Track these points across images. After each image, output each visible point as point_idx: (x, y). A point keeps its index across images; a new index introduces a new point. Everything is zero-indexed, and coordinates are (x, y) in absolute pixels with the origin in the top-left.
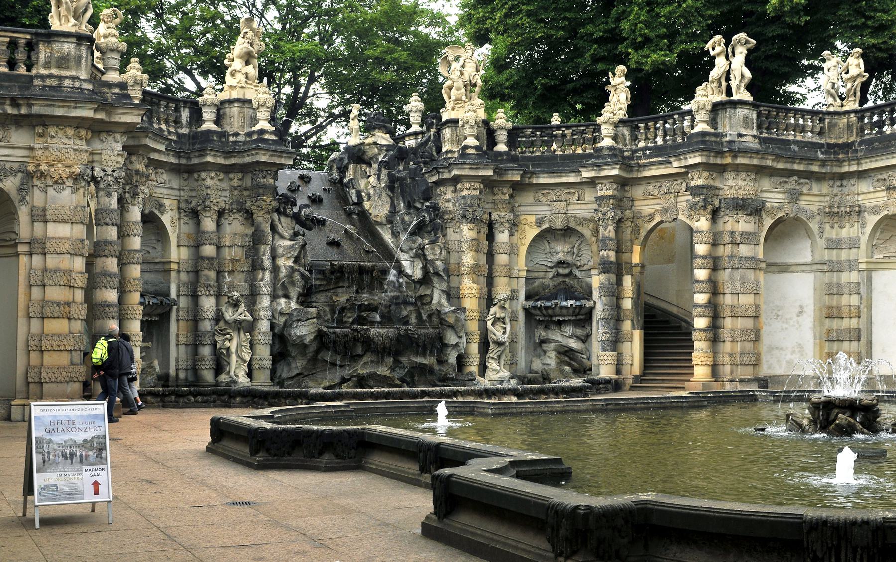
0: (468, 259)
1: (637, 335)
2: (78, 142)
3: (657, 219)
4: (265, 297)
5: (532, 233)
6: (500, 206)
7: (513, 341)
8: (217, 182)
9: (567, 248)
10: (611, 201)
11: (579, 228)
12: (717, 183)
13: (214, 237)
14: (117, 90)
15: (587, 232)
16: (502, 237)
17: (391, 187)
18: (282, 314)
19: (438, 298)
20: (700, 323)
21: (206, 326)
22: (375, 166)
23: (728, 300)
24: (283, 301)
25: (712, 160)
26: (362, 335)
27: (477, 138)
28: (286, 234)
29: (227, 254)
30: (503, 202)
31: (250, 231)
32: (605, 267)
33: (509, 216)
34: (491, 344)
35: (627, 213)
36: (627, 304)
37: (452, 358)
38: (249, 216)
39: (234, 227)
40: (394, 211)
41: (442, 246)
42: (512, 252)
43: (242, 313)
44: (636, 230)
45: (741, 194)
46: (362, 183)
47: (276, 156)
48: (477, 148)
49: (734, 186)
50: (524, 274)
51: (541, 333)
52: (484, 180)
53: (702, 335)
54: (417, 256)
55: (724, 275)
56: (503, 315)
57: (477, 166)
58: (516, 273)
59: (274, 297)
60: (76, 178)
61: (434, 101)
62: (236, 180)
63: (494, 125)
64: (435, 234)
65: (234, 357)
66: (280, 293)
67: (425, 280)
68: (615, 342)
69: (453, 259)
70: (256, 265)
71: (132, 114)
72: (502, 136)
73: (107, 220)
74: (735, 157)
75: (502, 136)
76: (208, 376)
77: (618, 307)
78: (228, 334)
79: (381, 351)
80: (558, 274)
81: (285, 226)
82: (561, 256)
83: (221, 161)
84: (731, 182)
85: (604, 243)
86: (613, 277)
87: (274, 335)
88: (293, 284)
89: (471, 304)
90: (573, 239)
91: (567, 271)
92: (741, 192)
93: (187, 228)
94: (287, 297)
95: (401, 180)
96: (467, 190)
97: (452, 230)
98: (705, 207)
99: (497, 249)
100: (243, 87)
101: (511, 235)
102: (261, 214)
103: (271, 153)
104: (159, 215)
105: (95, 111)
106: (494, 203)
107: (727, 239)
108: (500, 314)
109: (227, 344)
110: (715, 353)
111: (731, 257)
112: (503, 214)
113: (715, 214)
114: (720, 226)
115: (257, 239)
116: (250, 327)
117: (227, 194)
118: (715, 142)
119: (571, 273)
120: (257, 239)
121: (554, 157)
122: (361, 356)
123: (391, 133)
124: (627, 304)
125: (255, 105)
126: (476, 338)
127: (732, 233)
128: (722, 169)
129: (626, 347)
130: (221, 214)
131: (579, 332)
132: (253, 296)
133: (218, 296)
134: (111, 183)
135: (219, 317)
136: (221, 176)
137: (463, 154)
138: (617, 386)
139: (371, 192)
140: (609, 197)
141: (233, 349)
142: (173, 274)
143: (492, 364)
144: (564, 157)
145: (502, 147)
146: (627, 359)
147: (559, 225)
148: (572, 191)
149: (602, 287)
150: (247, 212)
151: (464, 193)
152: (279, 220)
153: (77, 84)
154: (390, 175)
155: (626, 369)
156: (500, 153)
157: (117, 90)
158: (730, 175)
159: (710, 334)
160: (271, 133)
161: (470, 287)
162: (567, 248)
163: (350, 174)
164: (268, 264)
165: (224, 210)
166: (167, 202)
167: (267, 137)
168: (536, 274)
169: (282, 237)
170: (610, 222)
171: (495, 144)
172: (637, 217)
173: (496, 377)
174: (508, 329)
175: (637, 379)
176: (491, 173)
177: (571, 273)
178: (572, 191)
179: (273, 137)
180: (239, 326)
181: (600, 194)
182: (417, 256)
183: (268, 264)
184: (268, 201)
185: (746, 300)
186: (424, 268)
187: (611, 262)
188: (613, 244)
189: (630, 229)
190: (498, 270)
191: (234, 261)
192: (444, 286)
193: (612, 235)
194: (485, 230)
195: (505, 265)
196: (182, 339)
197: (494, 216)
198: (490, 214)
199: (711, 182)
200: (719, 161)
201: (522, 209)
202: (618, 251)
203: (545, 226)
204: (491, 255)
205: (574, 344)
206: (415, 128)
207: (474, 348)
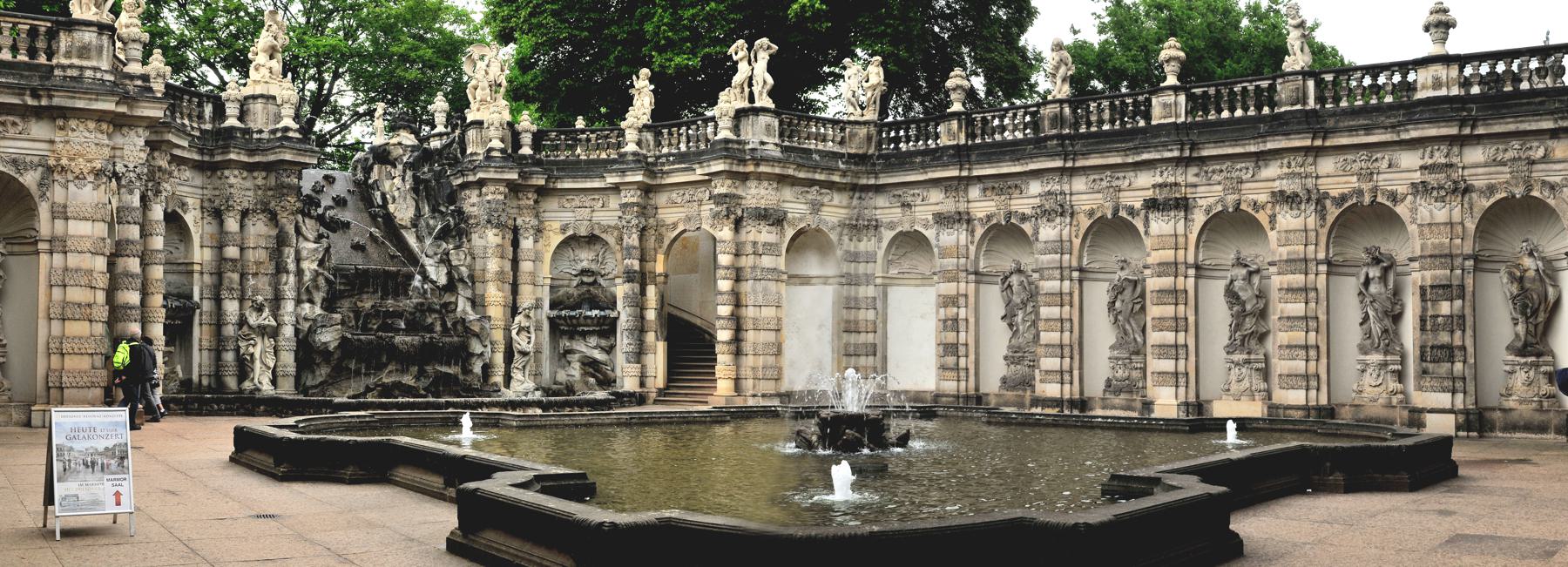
0: (493, 265)
1: (661, 347)
3: (681, 228)
5: (557, 239)
7: (538, 352)
9: (591, 255)
11: (603, 236)
12: (740, 192)
13: (238, 237)
15: (611, 240)
16: (527, 243)
17: (415, 190)
18: (306, 319)
19: (463, 305)
20: (724, 335)
21: (230, 330)
22: (400, 167)
23: (749, 312)
24: (307, 306)
27: (502, 140)
28: (311, 237)
29: (251, 256)
30: (528, 207)
31: (274, 232)
32: (630, 276)
33: (534, 222)
35: (651, 221)
36: (651, 315)
38: (273, 218)
39: (259, 229)
40: (418, 215)
42: (537, 259)
43: (266, 319)
44: (660, 239)
45: (763, 204)
46: (387, 185)
48: (503, 151)
49: (757, 195)
50: (548, 281)
51: (565, 343)
52: (510, 184)
53: (725, 348)
54: (441, 261)
55: (747, 287)
57: (501, 169)
59: (298, 302)
61: (459, 102)
63: (519, 127)
65: (258, 364)
66: (304, 297)
67: (451, 287)
68: (639, 354)
69: (479, 265)
70: (280, 269)
72: (527, 139)
75: (527, 139)
76: (232, 382)
77: (642, 317)
79: (404, 359)
80: (583, 283)
81: (310, 228)
82: (585, 264)
85: (628, 253)
86: (637, 287)
87: (299, 342)
88: (317, 288)
89: (496, 312)
90: (598, 247)
91: (591, 280)
93: (211, 228)
94: (311, 301)
95: (427, 181)
96: (493, 194)
98: (728, 217)
99: (521, 255)
101: (536, 241)
106: (519, 208)
107: (749, 249)
108: (525, 323)
109: (251, 350)
110: (738, 367)
111: (754, 268)
113: (738, 224)
114: (743, 236)
115: (281, 240)
116: (274, 333)
117: (250, 193)
119: (595, 282)
120: (281, 240)
121: (579, 162)
123: (416, 133)
124: (651, 315)
126: (501, 347)
127: (755, 243)
129: (649, 359)
130: (245, 214)
131: (603, 343)
132: (277, 300)
133: (242, 300)
135: (242, 322)
136: (245, 174)
137: (488, 158)
138: (641, 399)
139: (396, 194)
140: (633, 204)
141: (257, 355)
142: (196, 276)
144: (589, 162)
145: (526, 150)
146: (650, 372)
147: (583, 232)
149: (626, 297)
150: (271, 212)
151: (489, 197)
154: (414, 177)
155: (650, 382)
156: (524, 157)
159: (733, 347)
161: (495, 295)
162: (591, 255)
163: (374, 176)
164: (292, 267)
169: (306, 239)
171: (520, 147)
172: (660, 225)
173: (521, 388)
174: (533, 336)
175: (661, 392)
176: (515, 176)
177: (595, 282)
180: (262, 331)
181: (624, 200)
182: (441, 261)
183: (292, 267)
185: (768, 312)
186: (449, 274)
188: (637, 253)
191: (258, 263)
192: (469, 293)
193: (636, 243)
194: (510, 236)
196: (205, 344)
197: (519, 221)
202: (642, 260)
204: (515, 262)
205: (599, 355)
206: (440, 129)
207: (499, 358)
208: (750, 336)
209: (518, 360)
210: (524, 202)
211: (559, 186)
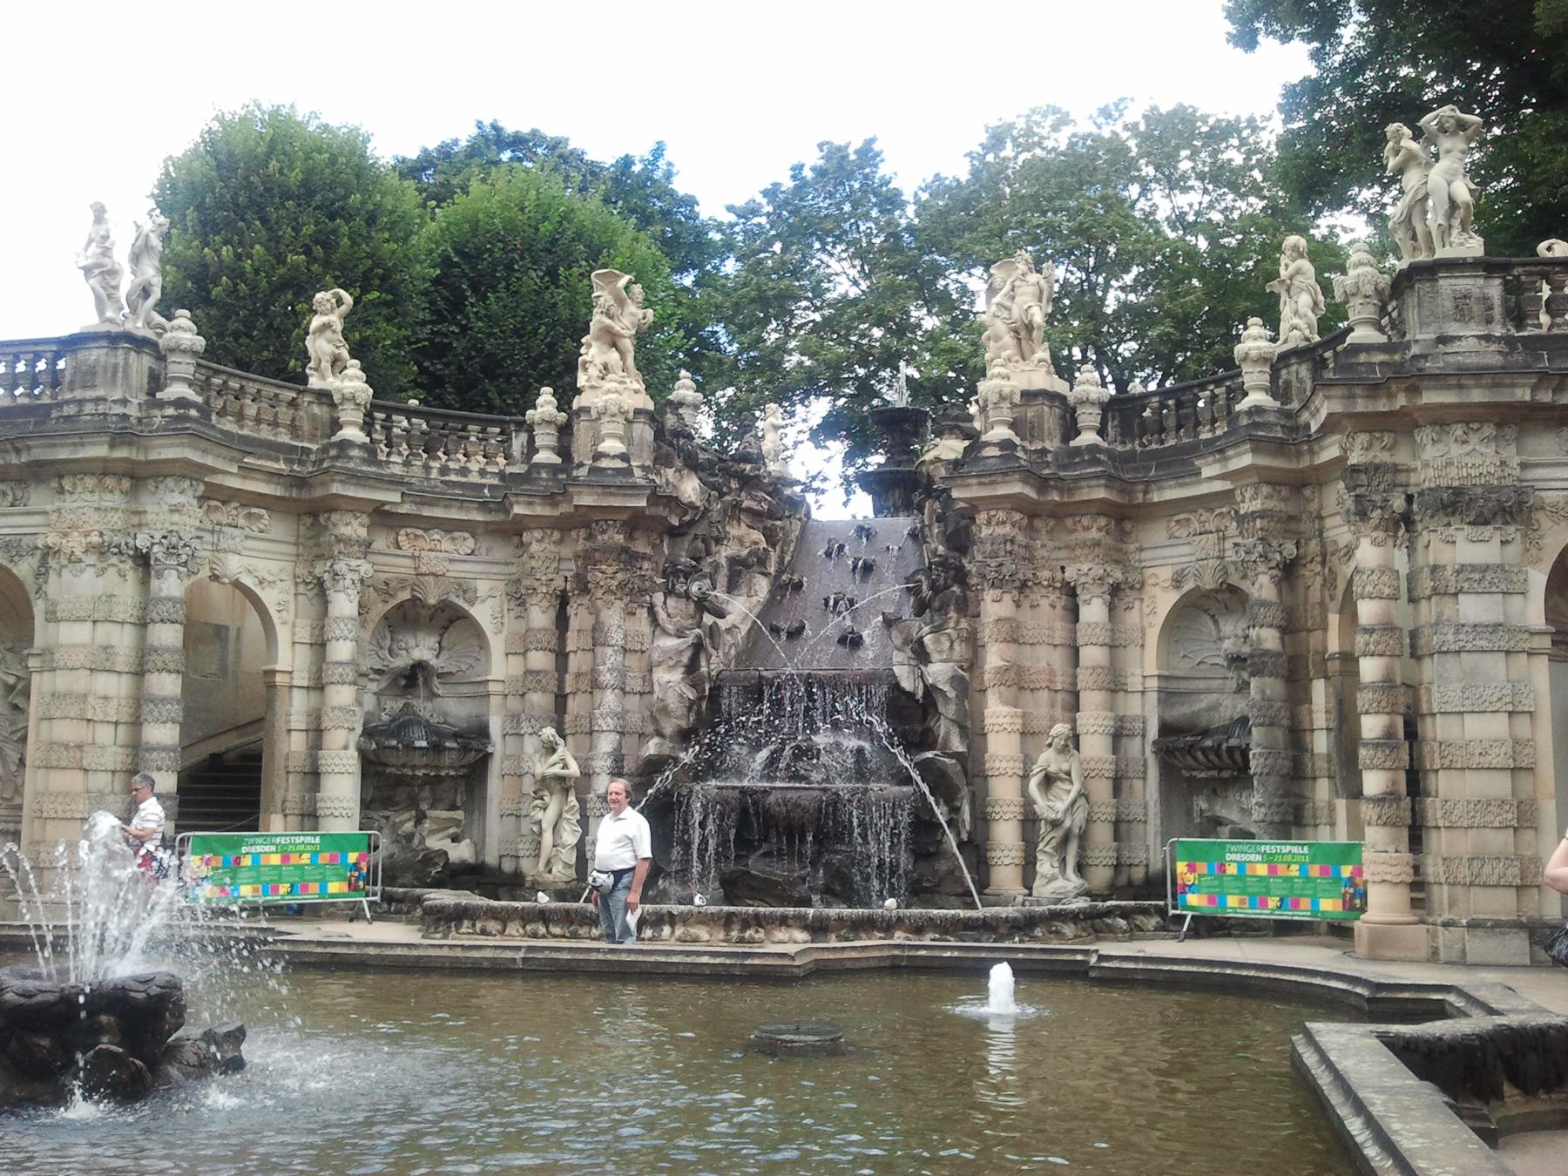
2: (108, 496)
4: (603, 736)
5: (1164, 600)
8: (552, 547)
10: (1258, 523)
12: (1402, 457)
14: (170, 411)
16: (1093, 611)
23: (1437, 729)
25: (1361, 406)
27: (1013, 426)
28: (670, 628)
41: (954, 635)
45: (1453, 477)
47: (611, 494)
49: (1447, 459)
50: (1153, 684)
56: (1065, 767)
58: (1135, 683)
60: (102, 550)
71: (172, 445)
72: (1089, 418)
73: (154, 615)
74: (1414, 390)
83: (546, 511)
84: (1430, 452)
92: (1453, 472)
100: (593, 387)
102: (599, 593)
103: (599, 490)
104: (466, 606)
105: (112, 446)
109: (539, 815)
112: (1085, 568)
118: (1381, 364)
125: (594, 414)
128: (1401, 425)
134: (159, 556)
136: (556, 535)
142: (495, 701)
143: (1045, 866)
147: (1209, 583)
148: (1224, 510)
153: (101, 409)
157: (170, 411)
158: (1425, 435)
160: (614, 457)
165: (564, 591)
166: (483, 587)
167: (604, 463)
168: (1201, 685)
169: (665, 632)
170: (1262, 568)
178: (1224, 510)
179: (619, 464)
180: (561, 784)
184: (610, 570)
187: (1266, 653)
189: (1319, 579)
195: (1094, 669)
198: (1063, 568)
199: (1384, 457)
200: (1382, 406)
201: (1145, 555)
203: (1189, 585)
208: (1446, 787)
210: (1081, 535)
211: (1156, 497)
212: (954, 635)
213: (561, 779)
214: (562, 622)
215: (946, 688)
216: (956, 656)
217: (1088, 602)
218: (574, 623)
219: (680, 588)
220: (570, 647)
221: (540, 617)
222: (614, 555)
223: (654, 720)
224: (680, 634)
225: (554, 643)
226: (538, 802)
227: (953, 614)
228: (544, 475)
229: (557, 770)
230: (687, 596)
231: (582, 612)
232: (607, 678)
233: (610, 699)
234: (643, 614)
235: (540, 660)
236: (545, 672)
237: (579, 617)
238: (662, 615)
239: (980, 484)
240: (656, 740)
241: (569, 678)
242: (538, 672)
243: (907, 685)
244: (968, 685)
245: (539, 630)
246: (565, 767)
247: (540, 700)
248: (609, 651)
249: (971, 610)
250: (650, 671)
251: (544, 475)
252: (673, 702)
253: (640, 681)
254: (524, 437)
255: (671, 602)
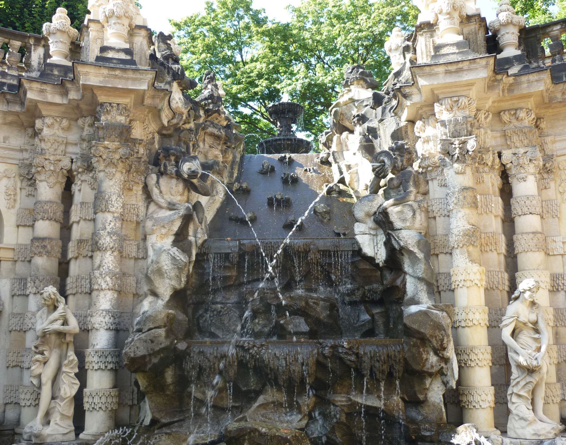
0: (460, 222)
4: (102, 294)
6: (515, 138)
8: (60, 133)
16: (526, 187)
26: (252, 356)
30: (520, 131)
34: (514, 370)
37: (435, 393)
41: (415, 205)
47: (116, 76)
62: (86, 128)
64: (405, 189)
69: (440, 225)
78: (42, 353)
88: (159, 272)
97: (436, 182)
99: (516, 207)
112: (522, 151)
122: (258, 393)
143: (519, 406)
152: (158, 182)
160: (119, 50)
165: (70, 171)
167: (110, 55)
169: (161, 207)
179: (123, 56)
190: (521, 243)
192: (421, 269)
194: (493, 181)
197: (507, 155)
204: (509, 222)
207: (481, 378)
209: (519, 385)
212: (415, 205)
213: (61, 334)
214: (67, 196)
215: (416, 250)
216: (417, 224)
217: (524, 180)
218: (78, 198)
219: (171, 169)
220: (74, 216)
221: (48, 191)
222: (118, 131)
223: (149, 280)
224: (172, 206)
225: (59, 215)
226: (38, 357)
227: (412, 189)
228: (56, 73)
229: (57, 326)
230: (179, 175)
231: (86, 188)
232: (106, 240)
233: (108, 260)
234: (138, 189)
235: (46, 228)
236: (50, 239)
237: (82, 192)
238: (155, 192)
239: (448, 72)
240: (150, 298)
241: (72, 246)
242: (43, 239)
243: (368, 250)
244: (433, 246)
245: (46, 202)
246: (65, 323)
247: (44, 263)
248: (109, 217)
249: (422, 189)
250: (145, 239)
251: (56, 73)
252: (166, 264)
253: (135, 248)
254: (40, 51)
255: (163, 181)
